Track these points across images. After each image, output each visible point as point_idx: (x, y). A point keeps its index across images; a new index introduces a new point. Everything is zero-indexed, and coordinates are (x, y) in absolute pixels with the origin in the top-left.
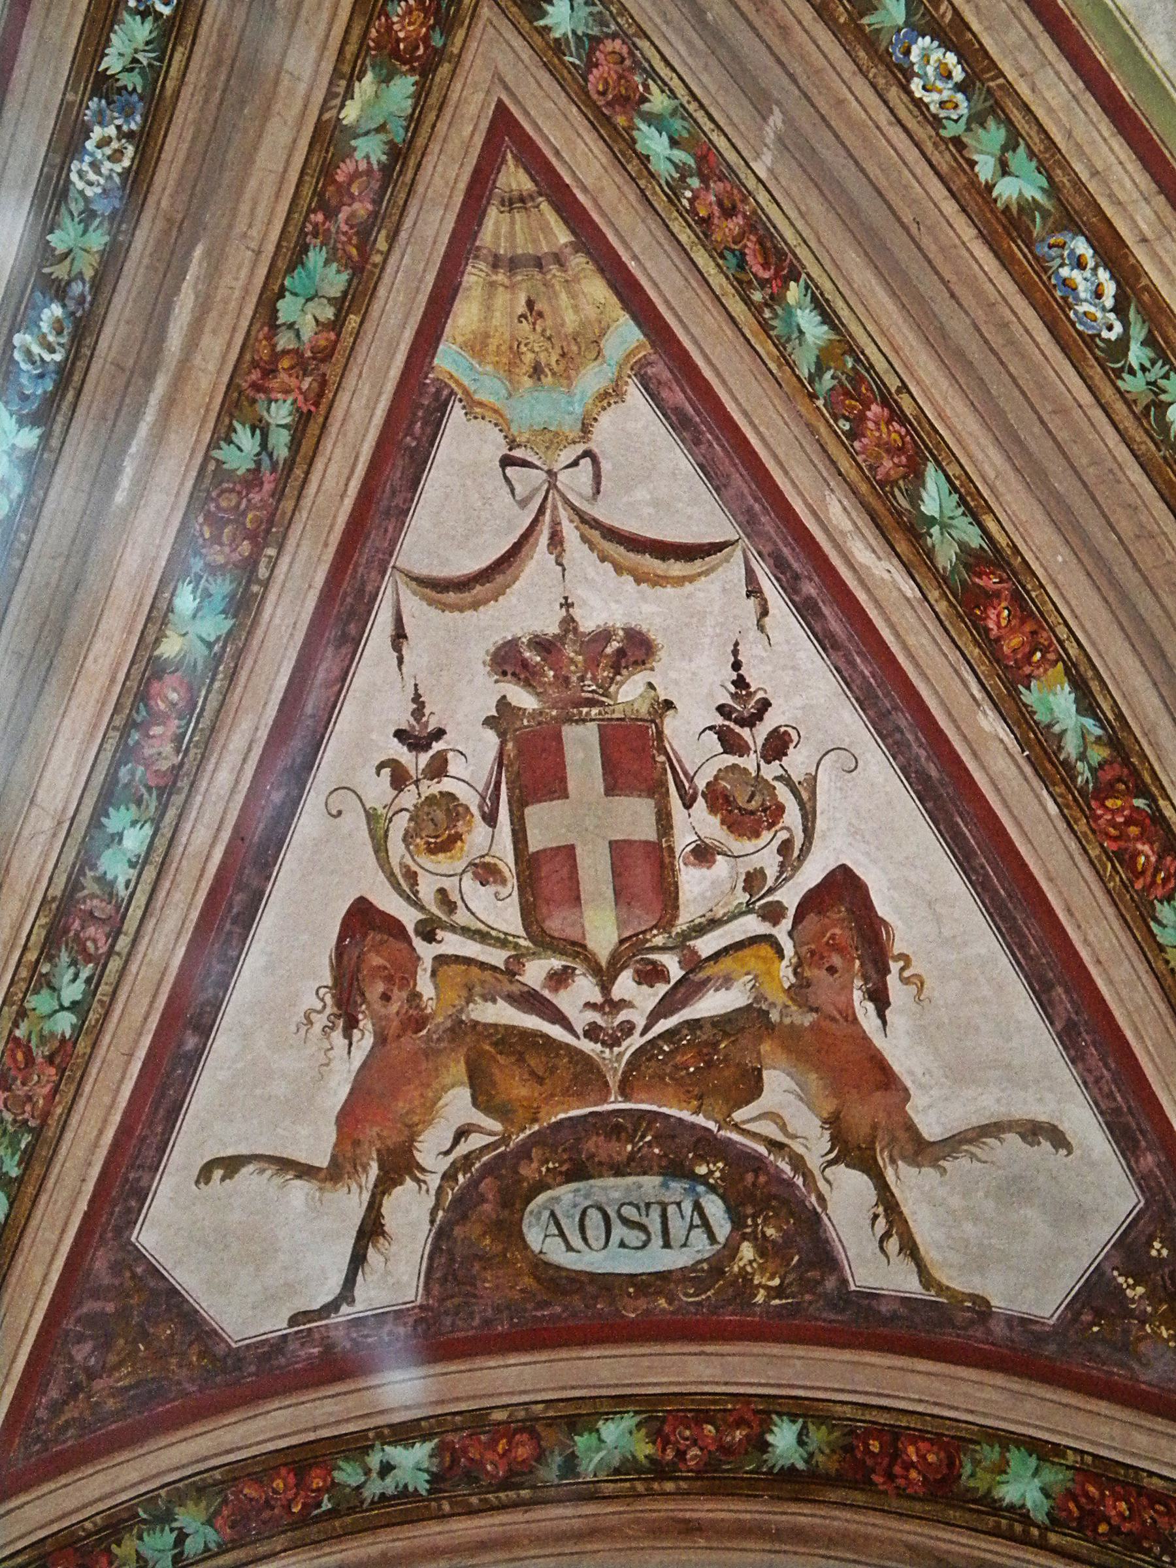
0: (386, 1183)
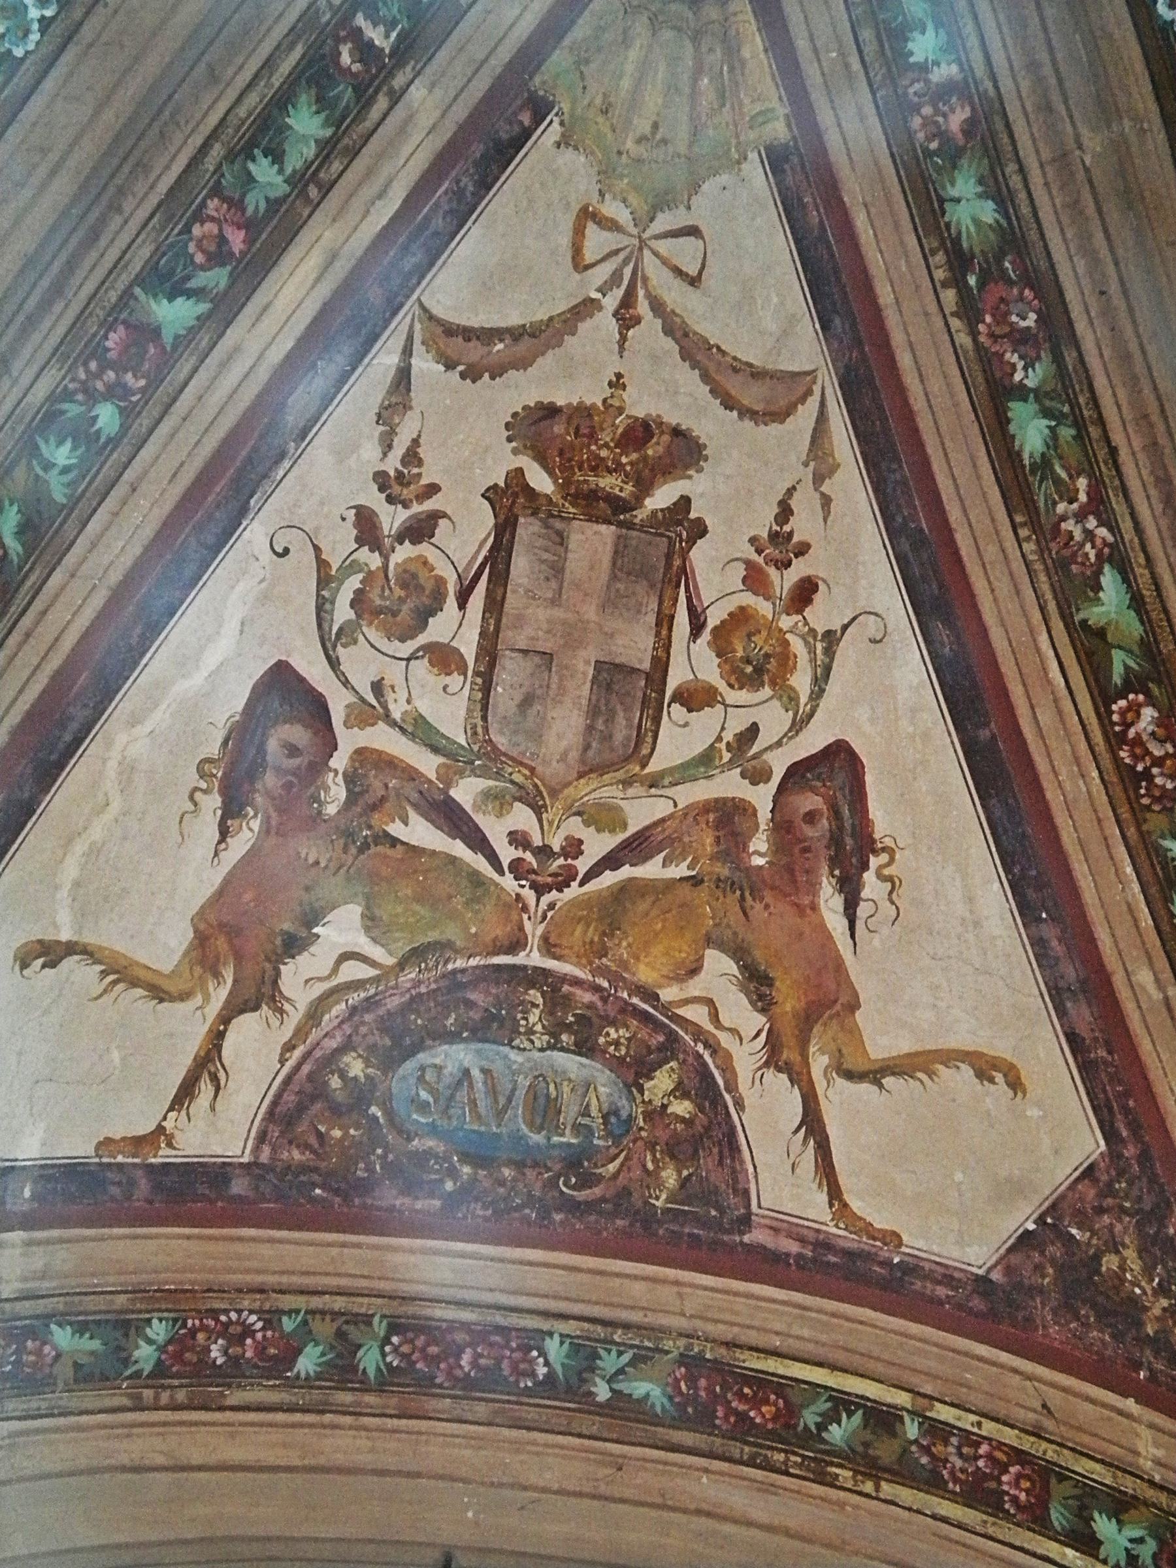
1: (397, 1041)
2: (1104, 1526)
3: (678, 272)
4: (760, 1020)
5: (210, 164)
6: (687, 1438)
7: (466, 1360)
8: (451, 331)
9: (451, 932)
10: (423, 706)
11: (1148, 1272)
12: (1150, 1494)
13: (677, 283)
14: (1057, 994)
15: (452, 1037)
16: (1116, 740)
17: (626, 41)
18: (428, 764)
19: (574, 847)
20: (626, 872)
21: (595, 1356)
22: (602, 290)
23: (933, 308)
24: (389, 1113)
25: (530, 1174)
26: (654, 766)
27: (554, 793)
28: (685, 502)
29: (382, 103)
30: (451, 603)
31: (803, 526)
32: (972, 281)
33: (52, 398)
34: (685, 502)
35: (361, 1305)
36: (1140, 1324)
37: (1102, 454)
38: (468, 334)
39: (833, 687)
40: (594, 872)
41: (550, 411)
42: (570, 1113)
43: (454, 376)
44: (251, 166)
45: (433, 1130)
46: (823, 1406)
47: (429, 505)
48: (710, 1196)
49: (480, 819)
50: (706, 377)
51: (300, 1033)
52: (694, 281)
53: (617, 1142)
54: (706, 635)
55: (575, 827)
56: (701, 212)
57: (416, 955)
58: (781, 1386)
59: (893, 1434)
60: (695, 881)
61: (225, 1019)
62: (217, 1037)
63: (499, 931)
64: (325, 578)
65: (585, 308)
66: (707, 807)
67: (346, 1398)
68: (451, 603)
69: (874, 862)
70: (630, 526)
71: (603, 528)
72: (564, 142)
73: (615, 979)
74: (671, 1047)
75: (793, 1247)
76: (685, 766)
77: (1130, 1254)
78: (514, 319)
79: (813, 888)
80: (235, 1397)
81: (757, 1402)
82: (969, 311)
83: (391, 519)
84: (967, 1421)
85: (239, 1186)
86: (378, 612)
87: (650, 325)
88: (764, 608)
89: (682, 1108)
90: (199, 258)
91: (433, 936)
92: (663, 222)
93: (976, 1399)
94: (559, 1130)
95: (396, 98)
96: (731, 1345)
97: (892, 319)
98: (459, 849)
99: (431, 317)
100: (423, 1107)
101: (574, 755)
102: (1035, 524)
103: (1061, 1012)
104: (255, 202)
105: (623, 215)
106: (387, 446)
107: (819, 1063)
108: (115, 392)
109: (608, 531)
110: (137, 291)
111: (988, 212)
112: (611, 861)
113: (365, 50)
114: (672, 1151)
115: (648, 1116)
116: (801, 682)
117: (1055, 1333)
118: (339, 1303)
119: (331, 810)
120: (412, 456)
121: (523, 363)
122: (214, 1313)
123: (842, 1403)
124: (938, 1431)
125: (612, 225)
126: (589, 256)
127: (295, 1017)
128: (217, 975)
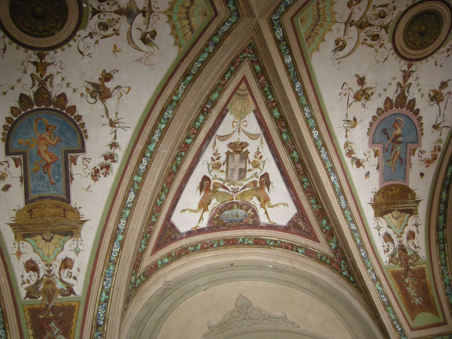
0: (204, 211)
1: (221, 212)
2: (299, 250)
3: (244, 126)
4: (260, 203)
5: (191, 124)
6: (255, 246)
7: (231, 242)
8: (220, 136)
9: (226, 199)
10: (220, 177)
11: (303, 224)
12: (304, 246)
13: (244, 127)
14: (292, 196)
15: (227, 210)
16: (296, 168)
17: (236, 102)
18: (221, 182)
19: (238, 188)
20: (244, 190)
21: (245, 239)
22: (236, 129)
23: (273, 124)
24: (221, 219)
25: (237, 223)
26: (246, 178)
27: (235, 183)
28: (247, 150)
29: (210, 113)
30: (222, 165)
31: (260, 150)
32: (277, 121)
33: (177, 153)
34: (247, 150)
35: (220, 239)
36: (302, 229)
37: (293, 139)
38: (222, 136)
39: (265, 167)
40: (240, 190)
41: (231, 143)
42: (240, 215)
43: (221, 141)
44: (196, 123)
45: (226, 220)
46: (269, 241)
47: (219, 156)
48: (256, 222)
49: (227, 187)
50: (248, 136)
51: (211, 213)
52: (246, 126)
53: (245, 217)
54: (251, 164)
55: (238, 186)
56: (247, 118)
57: (222, 202)
58: (264, 240)
59: (277, 243)
60: (251, 190)
61: (203, 213)
62: (202, 215)
63: (231, 198)
64: (208, 165)
65: (235, 131)
66: (252, 182)
67: (219, 248)
68: (222, 165)
69: (271, 184)
70: (241, 154)
71: (238, 154)
72: (230, 114)
73: (244, 201)
74: (250, 207)
75: (265, 226)
76: (249, 178)
77: (301, 222)
78: (226, 134)
79: (264, 188)
80: (208, 250)
81: (262, 241)
82: (277, 124)
83: (215, 158)
84: (285, 241)
85: (206, 229)
86: (214, 168)
87: (242, 132)
88: (257, 160)
89: (252, 213)
90: (191, 134)
91: (224, 200)
92: (242, 121)
93: (285, 238)
94: (239, 218)
95: (211, 113)
96: (259, 236)
97: (268, 126)
98: (226, 191)
99: (217, 135)
100: (224, 218)
101: (237, 178)
102: (286, 147)
103: (292, 198)
104: (197, 127)
105: (238, 121)
106: (214, 150)
107: (266, 206)
108: (183, 151)
109: (239, 155)
111: (278, 114)
112: (242, 189)
113: (207, 108)
114: (252, 218)
115: (249, 215)
116: (261, 166)
117: (293, 231)
118: (218, 239)
119: (212, 189)
120: (217, 151)
121: (228, 138)
122: (205, 243)
123: (271, 240)
124: (282, 242)
125: (237, 122)
126: (234, 126)
127: (210, 211)
128: (201, 209)
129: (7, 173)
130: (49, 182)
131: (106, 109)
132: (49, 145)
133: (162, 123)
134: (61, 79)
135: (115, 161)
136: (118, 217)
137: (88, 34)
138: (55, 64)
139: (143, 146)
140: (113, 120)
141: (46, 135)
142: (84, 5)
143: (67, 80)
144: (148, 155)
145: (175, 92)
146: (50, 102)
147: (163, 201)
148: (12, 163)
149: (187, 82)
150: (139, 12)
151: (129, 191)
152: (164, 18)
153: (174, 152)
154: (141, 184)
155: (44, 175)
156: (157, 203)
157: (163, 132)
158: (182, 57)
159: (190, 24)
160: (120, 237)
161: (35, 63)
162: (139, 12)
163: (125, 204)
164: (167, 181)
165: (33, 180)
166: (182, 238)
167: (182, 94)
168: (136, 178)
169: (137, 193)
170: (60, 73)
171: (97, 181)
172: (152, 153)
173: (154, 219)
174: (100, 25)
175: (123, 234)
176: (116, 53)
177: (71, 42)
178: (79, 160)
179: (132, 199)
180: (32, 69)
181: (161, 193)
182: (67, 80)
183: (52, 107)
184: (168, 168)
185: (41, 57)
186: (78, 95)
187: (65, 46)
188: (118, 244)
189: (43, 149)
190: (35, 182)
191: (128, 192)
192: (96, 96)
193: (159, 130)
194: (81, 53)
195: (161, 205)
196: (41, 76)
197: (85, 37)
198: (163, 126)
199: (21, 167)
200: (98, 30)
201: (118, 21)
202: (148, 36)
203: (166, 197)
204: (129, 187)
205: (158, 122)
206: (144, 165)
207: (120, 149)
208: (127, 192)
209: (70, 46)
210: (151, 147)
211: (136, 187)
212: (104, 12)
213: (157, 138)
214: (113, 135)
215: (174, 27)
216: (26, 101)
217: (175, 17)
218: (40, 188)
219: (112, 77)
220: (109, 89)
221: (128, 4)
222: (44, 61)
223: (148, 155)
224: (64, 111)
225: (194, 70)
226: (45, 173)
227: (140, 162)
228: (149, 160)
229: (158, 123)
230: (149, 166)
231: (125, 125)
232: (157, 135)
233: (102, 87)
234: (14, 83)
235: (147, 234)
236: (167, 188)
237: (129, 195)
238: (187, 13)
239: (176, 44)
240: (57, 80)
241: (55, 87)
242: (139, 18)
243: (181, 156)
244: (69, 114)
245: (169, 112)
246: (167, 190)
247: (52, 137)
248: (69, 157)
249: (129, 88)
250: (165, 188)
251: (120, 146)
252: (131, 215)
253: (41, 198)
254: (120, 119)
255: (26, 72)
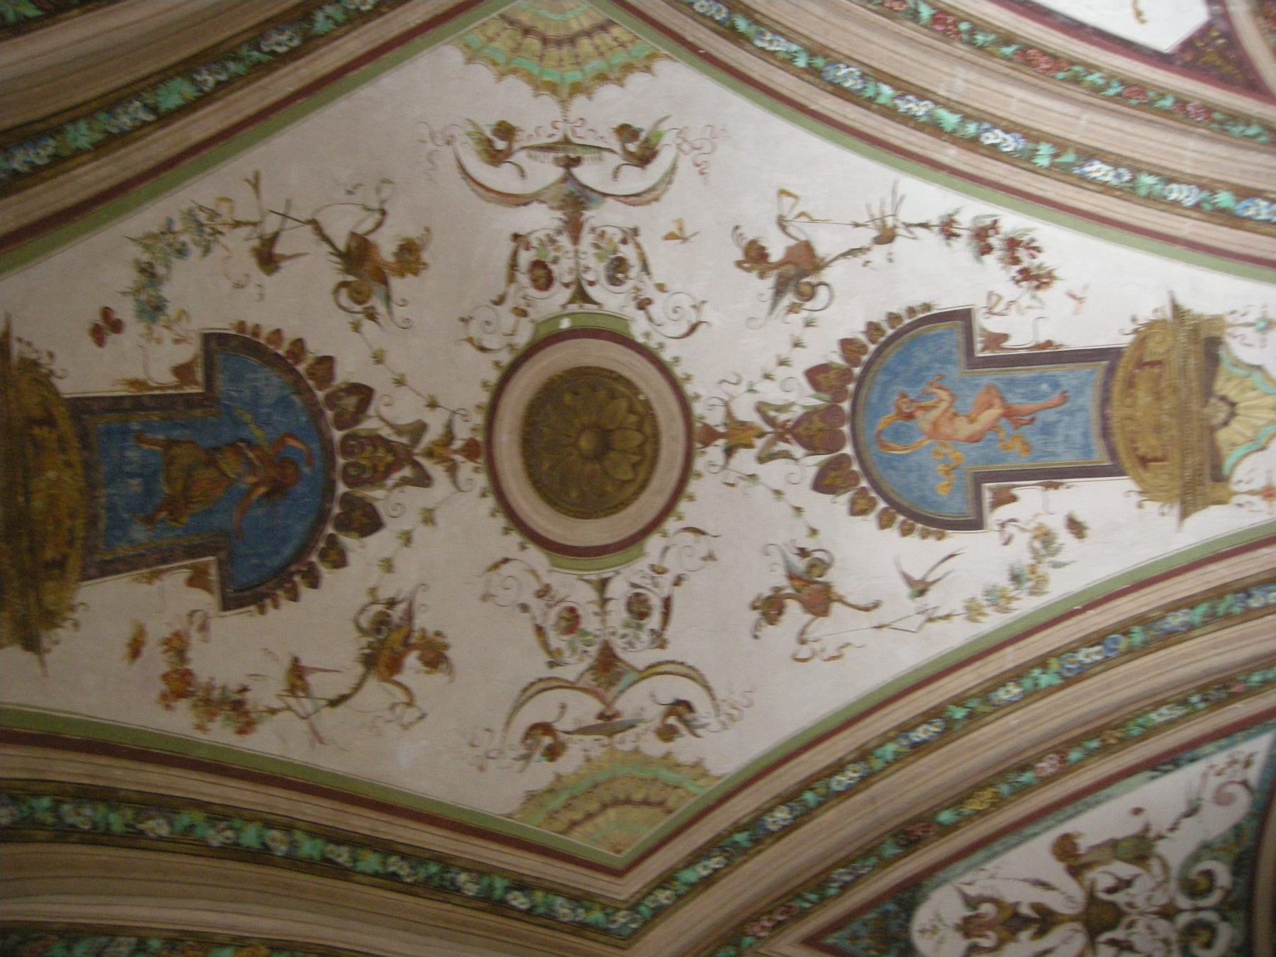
110: (921, 23)
129: (1033, 525)
130: (1059, 409)
131: (844, 255)
132: (953, 410)
133: (878, 94)
134: (767, 383)
135: (995, 222)
136: (1162, 207)
137: (641, 312)
138: (726, 398)
139: (945, 144)
140: (875, 233)
141: (924, 421)
142: (565, 324)
143: (771, 366)
144: (971, 128)
145: (783, 61)
146: (831, 412)
147: (1111, 77)
148: (1004, 512)
149: (754, 29)
150: (569, 177)
151: (1083, 178)
152: (580, 105)
153: (960, 53)
154: (1061, 145)
155: (1038, 423)
156: (1119, 95)
157: (903, 88)
158: (683, 50)
159: (588, 34)
160: (1224, 199)
161: (729, 452)
162: (569, 177)
163: (1120, 189)
164: (1048, 70)
165: (1054, 454)
166: (1226, 16)
167: (790, 40)
168: (1043, 161)
169: (1089, 154)
170: (751, 384)
171: (1056, 273)
172: (967, 118)
173: (1168, 103)
174: (614, 281)
175: (1213, 192)
176: (688, 232)
177: (666, 356)
178: (993, 325)
179: (1106, 168)
180: (745, 460)
181: (1086, 85)
182: (771, 366)
183: (846, 405)
184: (1007, 67)
185: (710, 436)
186: (808, 335)
187: (679, 371)
188: (1245, 203)
189: (964, 428)
190: (1060, 449)
191: (1084, 182)
192: (809, 284)
193: (898, 102)
194: (693, 328)
195: (1123, 82)
196: (762, 435)
197: (650, 319)
198: (886, 90)
199: (1014, 486)
200: (629, 285)
201: (598, 231)
202: (632, 147)
203: (1097, 68)
204: (1070, 179)
205: (874, 107)
206: (1005, 140)
207: (957, 212)
208: (1084, 185)
209: (677, 360)
210: (950, 120)
211: (1069, 158)
212: (579, 270)
213: (922, 103)
214: (919, 232)
215: (603, 78)
216: (833, 474)
217: (574, 76)
218: (1076, 434)
219: (753, 243)
220: (790, 250)
221: (552, 208)
222: (721, 430)
223: (971, 128)
224: (857, 371)
225: (719, 11)
226: (1033, 420)
227: (994, 152)
228: (986, 126)
229: (876, 104)
230: (1004, 123)
231: (889, 200)
232: (911, 105)
233: (783, 269)
234: (783, 509)
235: (1213, 121)
236: (1069, 70)
237: (1095, 178)
238: (559, 43)
239: (648, 69)
240: (771, 393)
241: (791, 397)
242: (588, 174)
243: (972, 32)
244: (865, 358)
245: (845, 77)
246: (1077, 68)
247: (929, 403)
248: (987, 354)
249: (783, 192)
250: (1069, 72)
251: (950, 212)
252: (1155, 170)
253: (1106, 433)
254: (871, 215)
255: (753, 477)
